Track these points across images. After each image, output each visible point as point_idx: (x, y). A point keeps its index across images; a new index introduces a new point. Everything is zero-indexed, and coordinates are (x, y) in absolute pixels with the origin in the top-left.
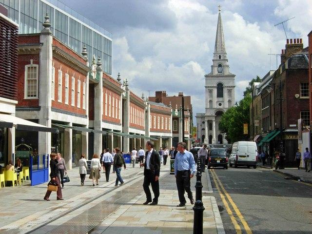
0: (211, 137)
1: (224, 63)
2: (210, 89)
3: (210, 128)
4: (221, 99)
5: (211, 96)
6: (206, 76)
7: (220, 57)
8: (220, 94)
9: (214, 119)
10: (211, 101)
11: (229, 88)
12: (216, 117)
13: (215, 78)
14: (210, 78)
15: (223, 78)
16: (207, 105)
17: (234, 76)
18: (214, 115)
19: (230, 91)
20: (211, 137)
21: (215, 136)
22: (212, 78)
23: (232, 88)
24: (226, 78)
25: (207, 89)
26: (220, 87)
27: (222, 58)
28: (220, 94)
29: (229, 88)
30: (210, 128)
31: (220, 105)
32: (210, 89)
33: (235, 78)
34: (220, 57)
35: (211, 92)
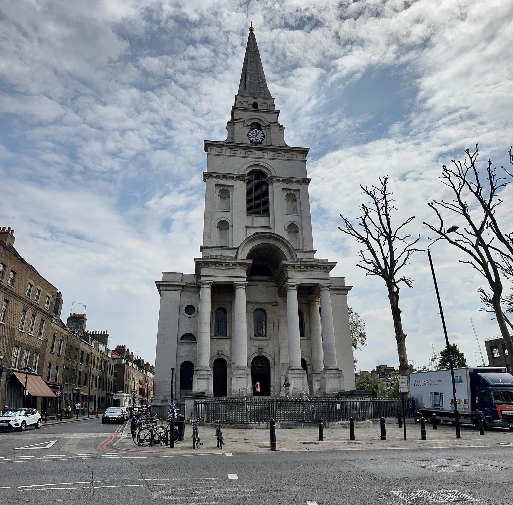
0: (221, 368)
1: (267, 118)
2: (223, 182)
3: (221, 326)
4: (261, 221)
5: (228, 209)
6: (208, 145)
7: (255, 105)
8: (258, 204)
9: (239, 276)
10: (223, 226)
13: (243, 152)
14: (225, 151)
15: (268, 155)
16: (207, 235)
17: (304, 152)
18: (243, 255)
19: (292, 197)
20: (221, 368)
21: (331, 315)
22: (233, 152)
23: (297, 186)
25: (213, 182)
26: (258, 186)
28: (258, 204)
29: (288, 186)
30: (221, 326)
32: (223, 182)
34: (255, 105)
35: (225, 193)
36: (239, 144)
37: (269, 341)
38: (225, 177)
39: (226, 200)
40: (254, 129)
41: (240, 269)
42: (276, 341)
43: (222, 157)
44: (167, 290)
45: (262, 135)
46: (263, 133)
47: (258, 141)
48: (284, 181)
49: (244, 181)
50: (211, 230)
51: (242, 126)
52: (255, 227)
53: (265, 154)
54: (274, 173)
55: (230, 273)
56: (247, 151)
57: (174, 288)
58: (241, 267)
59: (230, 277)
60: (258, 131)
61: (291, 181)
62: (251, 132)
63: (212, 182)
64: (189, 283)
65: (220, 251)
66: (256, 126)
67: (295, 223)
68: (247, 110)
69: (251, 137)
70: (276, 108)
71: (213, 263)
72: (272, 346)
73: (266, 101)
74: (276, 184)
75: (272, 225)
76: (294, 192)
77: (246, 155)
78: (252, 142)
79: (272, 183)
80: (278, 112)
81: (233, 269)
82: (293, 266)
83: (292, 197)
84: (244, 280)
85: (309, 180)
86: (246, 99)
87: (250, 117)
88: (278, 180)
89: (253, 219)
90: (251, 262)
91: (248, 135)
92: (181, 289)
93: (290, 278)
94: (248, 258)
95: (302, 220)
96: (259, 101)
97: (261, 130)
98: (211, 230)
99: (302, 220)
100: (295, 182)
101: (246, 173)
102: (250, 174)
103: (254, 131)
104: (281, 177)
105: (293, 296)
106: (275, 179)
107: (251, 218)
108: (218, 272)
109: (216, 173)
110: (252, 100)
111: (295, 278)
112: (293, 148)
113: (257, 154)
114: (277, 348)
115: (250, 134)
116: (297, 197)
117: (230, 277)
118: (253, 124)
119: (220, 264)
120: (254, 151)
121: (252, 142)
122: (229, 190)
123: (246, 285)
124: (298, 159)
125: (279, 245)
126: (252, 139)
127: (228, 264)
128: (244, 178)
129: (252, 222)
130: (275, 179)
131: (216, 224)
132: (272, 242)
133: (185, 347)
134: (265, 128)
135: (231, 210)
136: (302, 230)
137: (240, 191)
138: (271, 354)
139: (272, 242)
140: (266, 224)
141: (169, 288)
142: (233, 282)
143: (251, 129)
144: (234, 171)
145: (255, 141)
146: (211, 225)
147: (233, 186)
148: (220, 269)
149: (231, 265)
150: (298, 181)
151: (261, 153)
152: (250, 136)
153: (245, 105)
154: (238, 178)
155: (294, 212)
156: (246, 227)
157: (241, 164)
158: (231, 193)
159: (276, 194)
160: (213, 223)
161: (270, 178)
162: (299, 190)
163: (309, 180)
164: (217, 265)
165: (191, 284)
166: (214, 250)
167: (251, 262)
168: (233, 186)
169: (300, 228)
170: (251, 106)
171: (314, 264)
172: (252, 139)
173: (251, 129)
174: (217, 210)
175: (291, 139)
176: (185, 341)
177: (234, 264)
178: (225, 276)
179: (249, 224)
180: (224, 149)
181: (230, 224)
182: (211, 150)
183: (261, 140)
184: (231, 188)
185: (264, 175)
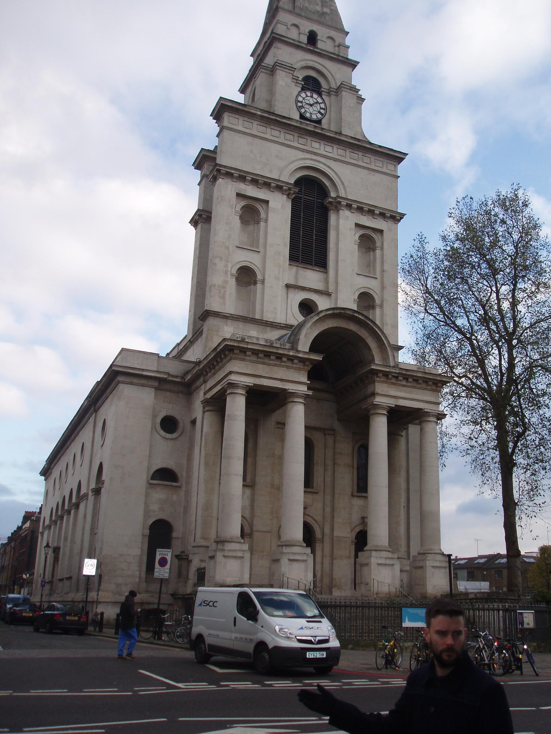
1: (334, 72)
2: (251, 191)
4: (311, 278)
5: (253, 245)
7: (312, 38)
9: (296, 381)
11: (366, 221)
12: (316, 373)
19: (368, 241)
24: (348, 155)
27: (320, 45)
29: (366, 221)
31: (307, 307)
32: (251, 191)
33: (402, 169)
34: (312, 38)
36: (284, 117)
37: (315, 496)
38: (255, 181)
39: (251, 228)
40: (309, 89)
41: (299, 369)
42: (328, 498)
43: (249, 139)
44: (131, 383)
45: (323, 106)
46: (324, 102)
47: (314, 117)
48: (360, 209)
49: (288, 195)
50: (226, 282)
51: (289, 80)
52: (303, 289)
53: (329, 149)
54: (343, 191)
55: (281, 373)
56: (296, 135)
57: (143, 381)
58: (301, 365)
59: (281, 380)
60: (315, 96)
61: (371, 212)
62: (303, 95)
63: (230, 187)
64: (172, 376)
65: (241, 325)
66: (311, 84)
67: (371, 292)
68: (297, 46)
69: (302, 107)
70: (352, 55)
71: (255, 352)
72: (319, 505)
73: (333, 34)
74: (345, 213)
75: (331, 289)
76: (373, 235)
77: (295, 144)
78: (302, 117)
79: (337, 210)
80: (353, 65)
81: (288, 367)
82: (386, 375)
83: (368, 241)
84: (303, 389)
85: (402, 216)
86: (297, 20)
87: (303, 64)
88: (349, 206)
89: (297, 273)
90: (318, 357)
91: (297, 101)
92: (156, 384)
93: (378, 394)
94: (314, 348)
95: (383, 288)
96: (322, 32)
97: (320, 94)
98: (226, 282)
99: (383, 288)
100: (377, 215)
101: (292, 182)
102: (298, 182)
103: (309, 94)
104: (356, 201)
105: (380, 427)
106: (344, 203)
107: (294, 269)
108: (261, 369)
109: (240, 171)
110: (307, 26)
111: (387, 395)
112: (380, 147)
113: (316, 145)
114: (328, 510)
115: (300, 99)
116: (378, 244)
117: (281, 380)
118: (307, 79)
119: (267, 355)
120: (309, 139)
121: (302, 117)
122: (260, 209)
123: (306, 397)
124: (384, 170)
125: (364, 334)
126: (303, 110)
127: (279, 357)
128: (290, 189)
129: (296, 278)
130: (344, 203)
131: (234, 271)
132: (353, 327)
133: (159, 494)
134: (329, 93)
135: (261, 249)
136: (381, 306)
137: (279, 212)
138: (319, 518)
139: (353, 327)
140: (319, 286)
141: (135, 380)
142: (285, 390)
143: (303, 89)
144: (271, 171)
145: (308, 115)
146: (226, 272)
147: (267, 202)
148: (264, 363)
149: (284, 359)
150: (382, 215)
151: (309, 141)
152: (300, 104)
153: (293, 34)
154: (279, 188)
155: (368, 268)
156: (288, 286)
157: (283, 159)
158: (263, 215)
159: (343, 230)
160: (229, 269)
161: (335, 199)
162: (381, 232)
163: (402, 216)
164: (261, 355)
165: (176, 377)
166: (229, 322)
167: (318, 357)
168: (267, 202)
169: (378, 301)
170: (304, 39)
171: (420, 375)
172: (303, 110)
173: (303, 89)
174: (237, 243)
175: (375, 127)
176: (160, 482)
177: (291, 359)
178: (273, 377)
179: (292, 282)
180: (255, 123)
181: (259, 277)
182: (227, 119)
183: (319, 116)
184: (264, 206)
185: (323, 191)
